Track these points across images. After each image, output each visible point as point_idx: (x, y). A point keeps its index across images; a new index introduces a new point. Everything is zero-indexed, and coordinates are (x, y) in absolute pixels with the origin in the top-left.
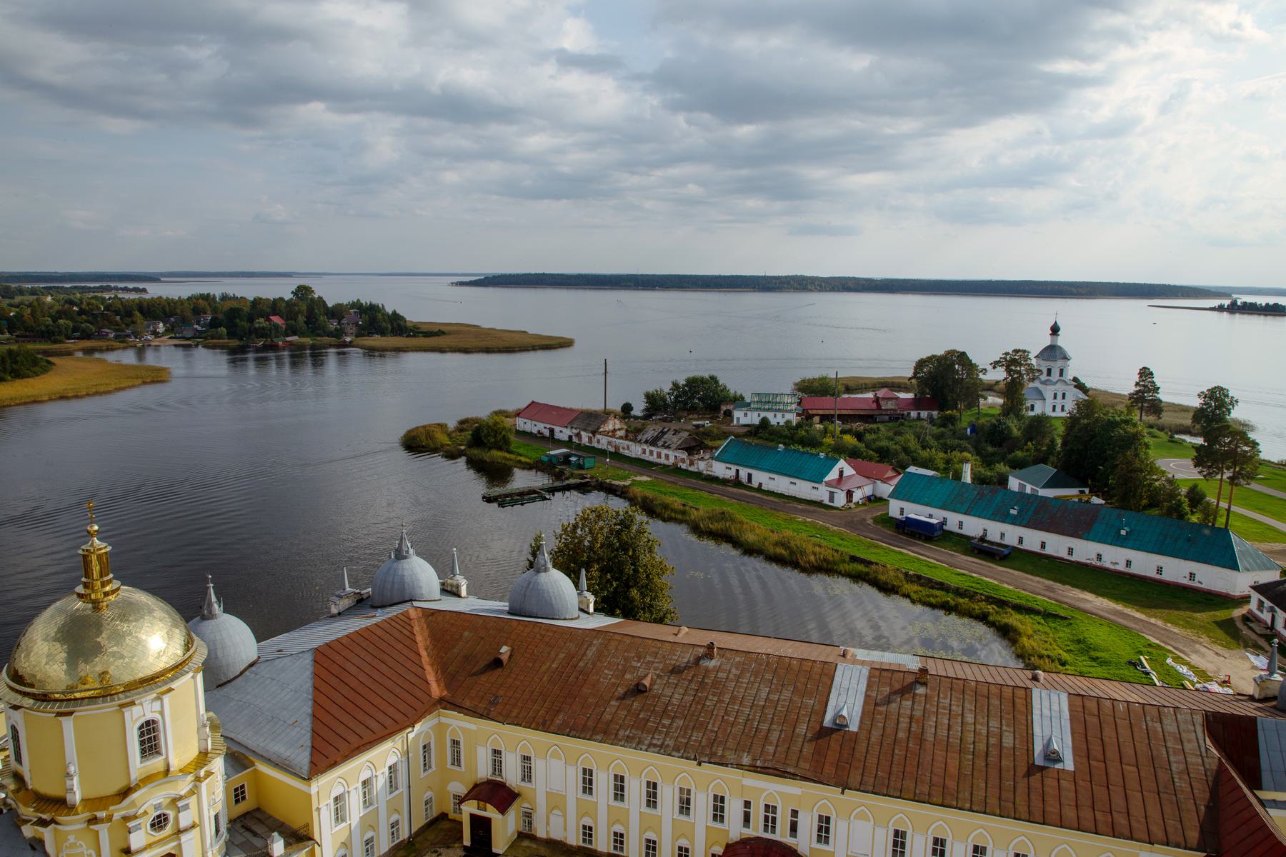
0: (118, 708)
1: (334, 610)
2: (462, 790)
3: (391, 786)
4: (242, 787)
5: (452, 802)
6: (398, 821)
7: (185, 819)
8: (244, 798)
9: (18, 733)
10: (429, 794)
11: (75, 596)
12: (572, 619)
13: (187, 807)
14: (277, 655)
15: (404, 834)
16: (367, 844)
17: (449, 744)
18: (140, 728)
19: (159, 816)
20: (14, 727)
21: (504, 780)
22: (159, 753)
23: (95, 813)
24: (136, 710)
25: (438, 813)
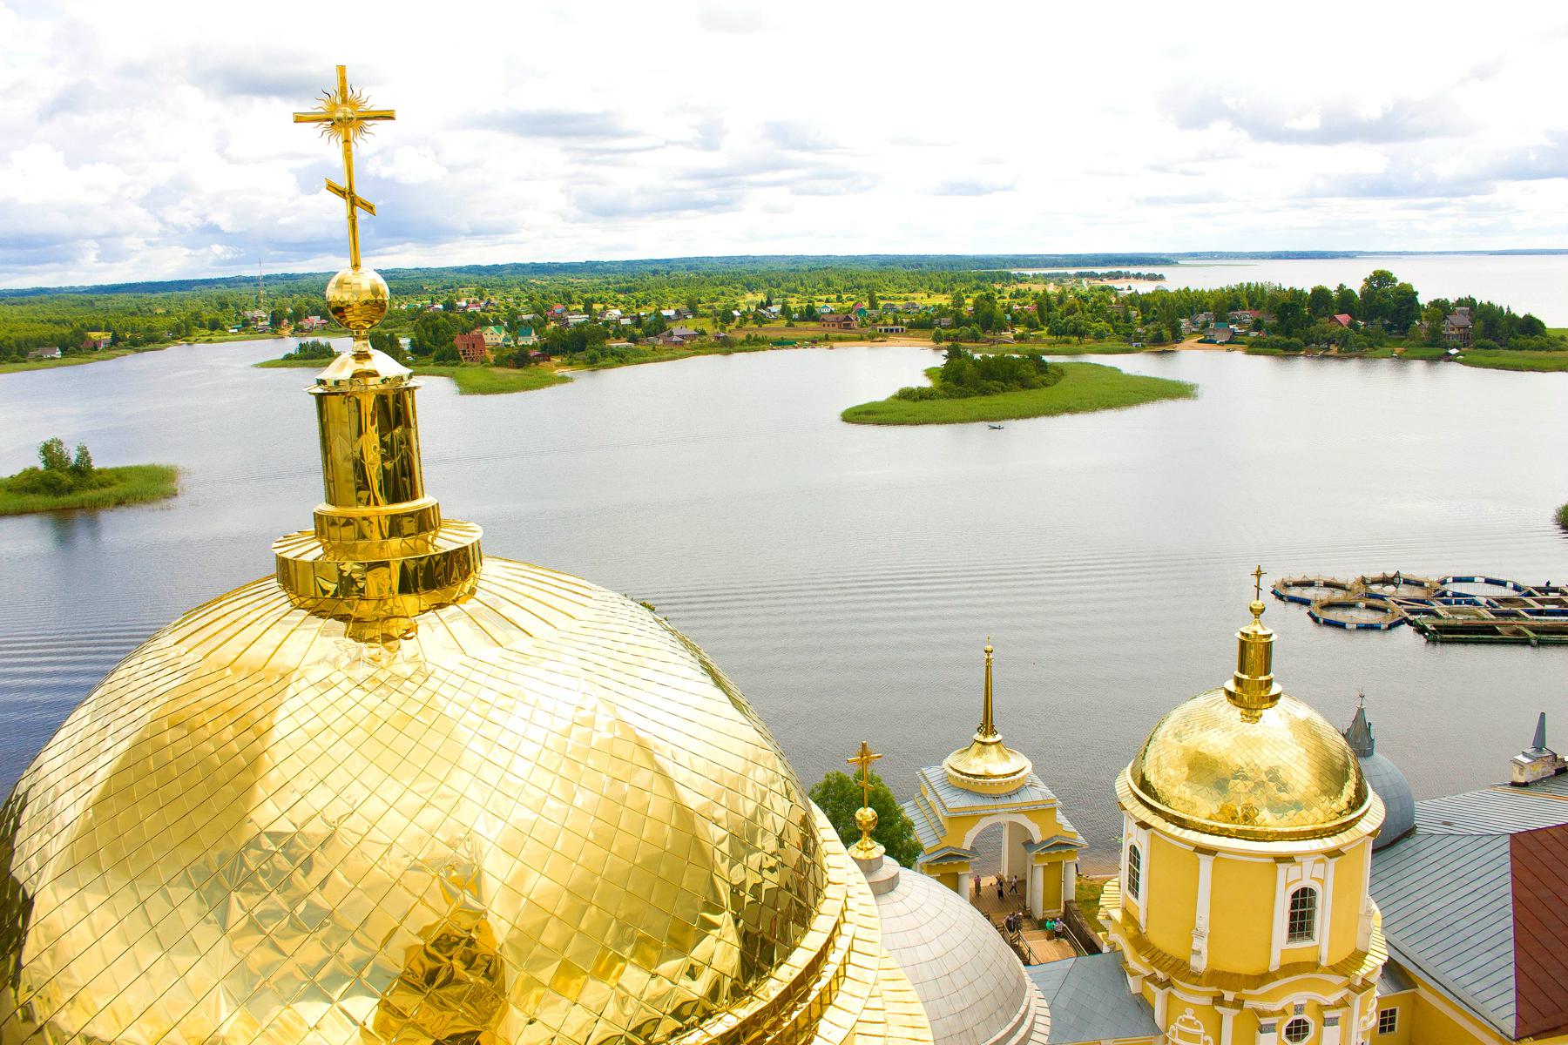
0: (1272, 861)
4: (1393, 1012)
8: (1392, 1028)
9: (1139, 857)
13: (1333, 1022)
14: (1445, 829)
18: (1293, 896)
19: (1298, 1022)
20: (1135, 847)
22: (1310, 936)
23: (1223, 991)
24: (1294, 871)
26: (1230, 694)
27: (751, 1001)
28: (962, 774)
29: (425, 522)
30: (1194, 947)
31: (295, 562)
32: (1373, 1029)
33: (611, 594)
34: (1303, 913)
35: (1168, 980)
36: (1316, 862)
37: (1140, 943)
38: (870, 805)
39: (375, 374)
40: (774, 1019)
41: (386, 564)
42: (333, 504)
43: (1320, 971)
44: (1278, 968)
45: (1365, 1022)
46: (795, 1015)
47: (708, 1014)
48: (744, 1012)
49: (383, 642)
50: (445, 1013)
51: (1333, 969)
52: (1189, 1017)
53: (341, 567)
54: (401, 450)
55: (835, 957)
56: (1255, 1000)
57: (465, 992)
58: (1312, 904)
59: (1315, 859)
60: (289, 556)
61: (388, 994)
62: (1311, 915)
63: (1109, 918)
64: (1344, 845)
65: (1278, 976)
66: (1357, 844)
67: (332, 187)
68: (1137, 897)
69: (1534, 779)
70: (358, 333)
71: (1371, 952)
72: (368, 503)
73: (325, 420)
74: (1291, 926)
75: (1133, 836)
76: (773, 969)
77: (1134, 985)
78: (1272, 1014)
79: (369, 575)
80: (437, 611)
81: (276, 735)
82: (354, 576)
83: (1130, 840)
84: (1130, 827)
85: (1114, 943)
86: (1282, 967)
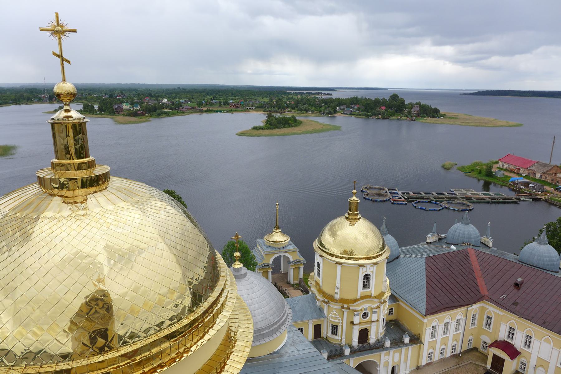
0: (358, 266)
1: (428, 241)
2: (489, 342)
3: (456, 329)
4: (392, 309)
5: (481, 344)
6: (456, 345)
7: (375, 317)
8: (392, 314)
10: (470, 337)
11: (344, 218)
12: (555, 272)
13: (375, 312)
15: (458, 351)
16: (441, 350)
17: (485, 317)
18: (364, 276)
19: (365, 313)
21: (513, 343)
24: (364, 269)
25: (473, 347)
26: (346, 217)
27: (195, 314)
28: (269, 241)
29: (91, 165)
30: (336, 292)
31: (44, 178)
32: (387, 314)
33: (153, 188)
34: (367, 281)
35: (328, 301)
36: (370, 266)
37: (321, 291)
38: (239, 251)
39: (71, 117)
40: (202, 319)
41: (76, 179)
42: (58, 159)
43: (371, 298)
44: (360, 297)
45: (384, 312)
46: (209, 318)
47: (181, 319)
48: (192, 318)
49: (74, 204)
50: (92, 323)
51: (375, 297)
52: (335, 312)
53: (60, 180)
54: (81, 142)
55: (222, 300)
56: (353, 307)
57: (99, 317)
58: (369, 278)
59: (371, 265)
60: (42, 176)
61: (72, 318)
62: (369, 281)
63: (311, 284)
64: (378, 261)
65: (360, 300)
66: (382, 261)
67: (54, 54)
68: (319, 277)
69: (433, 241)
70: (65, 103)
71: (386, 292)
72: (70, 159)
73: (54, 132)
74: (363, 285)
75: (318, 259)
76: (202, 303)
77: (318, 303)
78: (358, 311)
79: (70, 182)
80: (93, 194)
81: (34, 235)
82: (65, 183)
83: (318, 260)
84: (317, 256)
85: (313, 291)
86: (361, 297)
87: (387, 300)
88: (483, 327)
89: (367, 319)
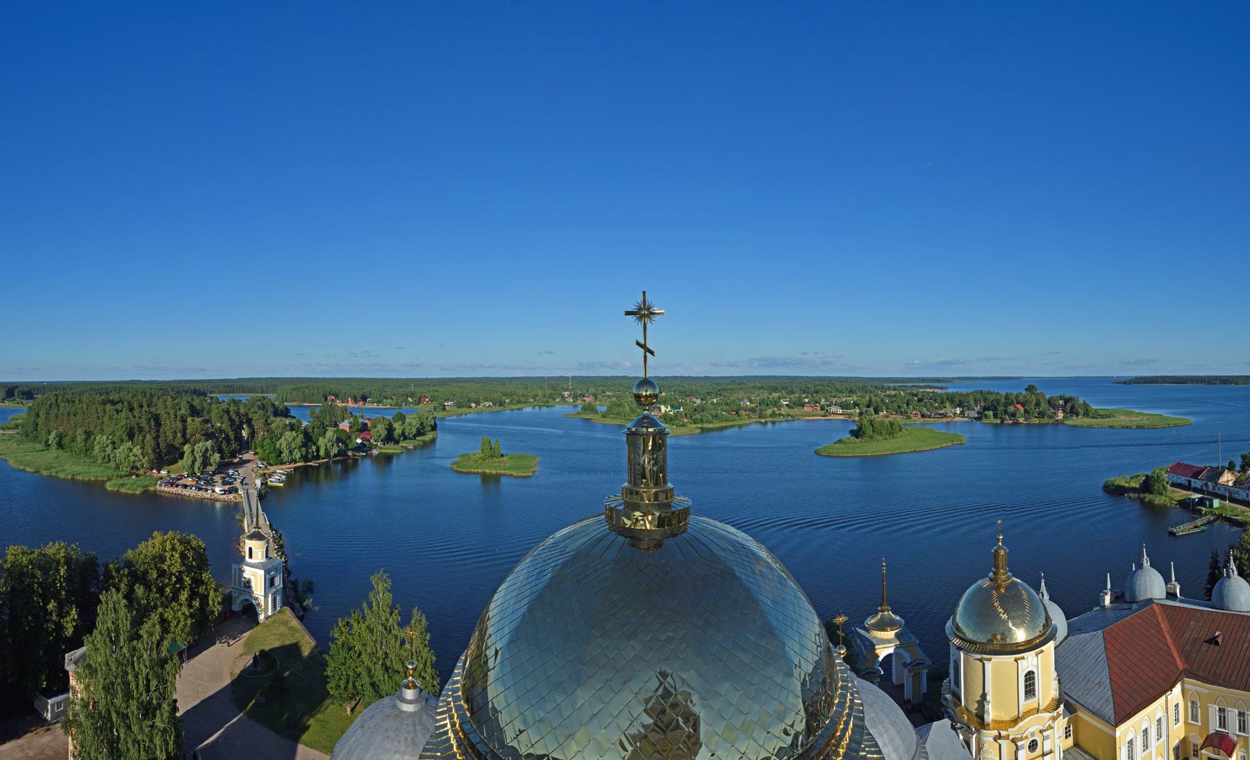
19: (1033, 741)
87: (1061, 713)
88: (1190, 721)
89: (1038, 751)
